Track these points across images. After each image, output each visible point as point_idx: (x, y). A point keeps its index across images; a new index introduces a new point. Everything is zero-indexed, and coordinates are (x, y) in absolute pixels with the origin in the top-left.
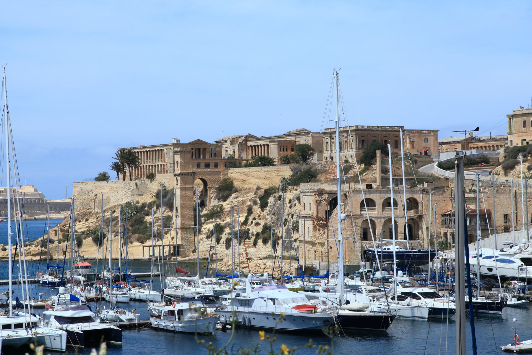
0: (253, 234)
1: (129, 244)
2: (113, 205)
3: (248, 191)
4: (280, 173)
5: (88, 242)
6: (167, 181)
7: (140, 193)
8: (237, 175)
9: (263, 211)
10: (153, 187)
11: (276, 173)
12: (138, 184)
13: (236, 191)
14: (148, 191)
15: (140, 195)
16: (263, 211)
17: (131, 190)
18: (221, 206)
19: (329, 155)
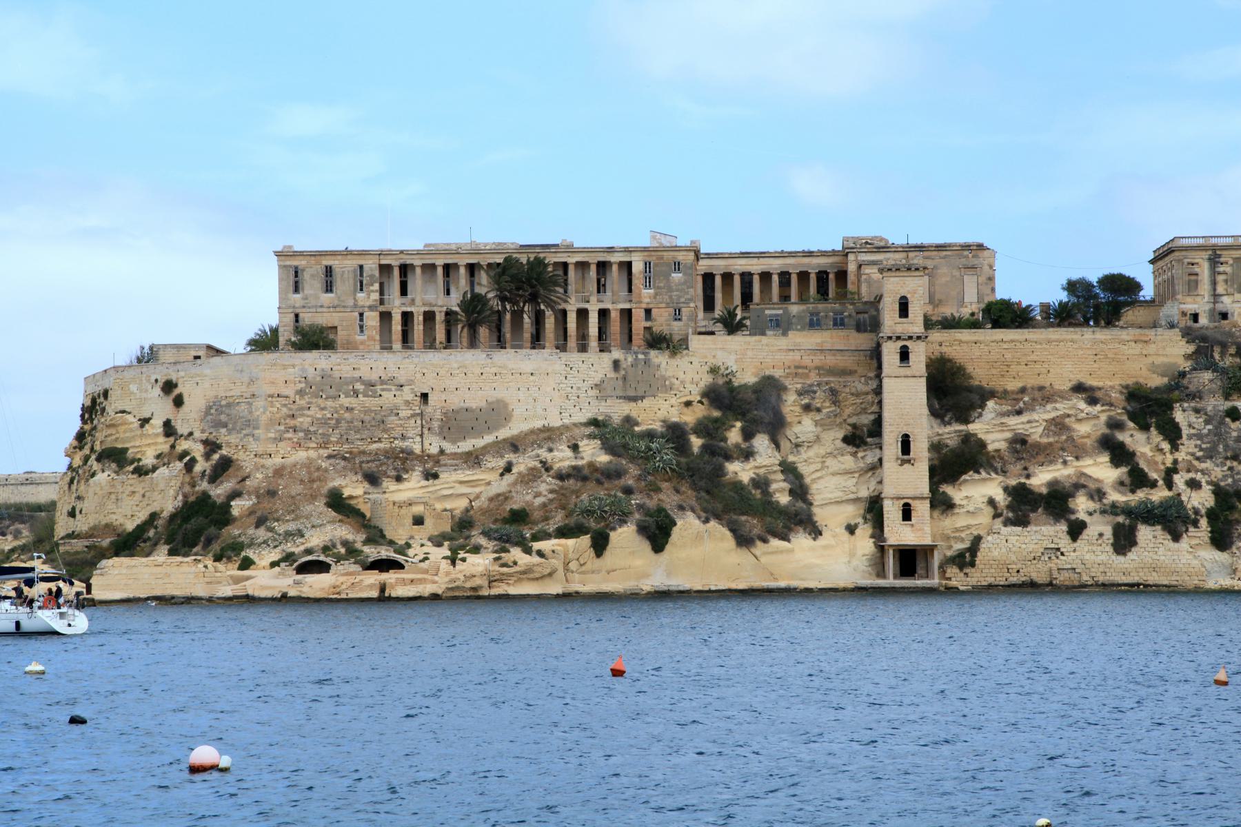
0: (1196, 512)
1: (759, 543)
2: (525, 427)
3: (1045, 395)
4: (1152, 348)
5: (625, 537)
6: (733, 357)
7: (631, 393)
8: (965, 346)
9: (1177, 450)
10: (681, 376)
11: (1136, 349)
12: (623, 365)
13: (985, 395)
14: (663, 386)
15: (634, 399)
16: (1177, 450)
17: (597, 380)
18: (967, 438)
19: (1208, 307)
